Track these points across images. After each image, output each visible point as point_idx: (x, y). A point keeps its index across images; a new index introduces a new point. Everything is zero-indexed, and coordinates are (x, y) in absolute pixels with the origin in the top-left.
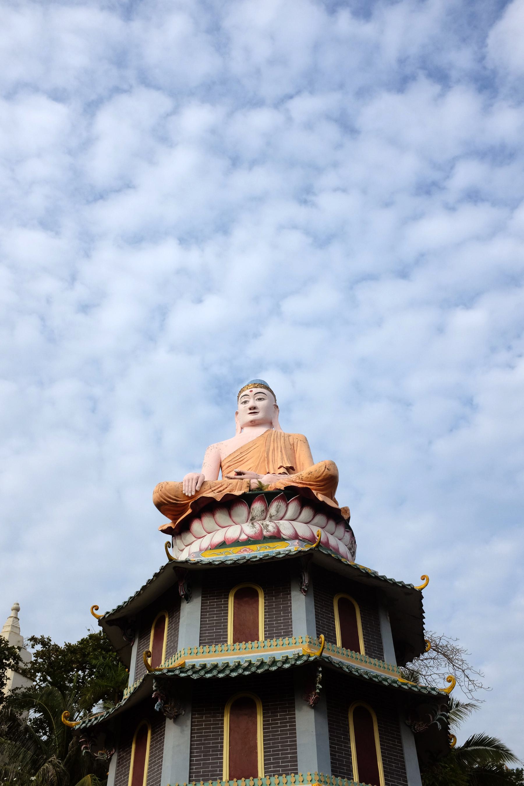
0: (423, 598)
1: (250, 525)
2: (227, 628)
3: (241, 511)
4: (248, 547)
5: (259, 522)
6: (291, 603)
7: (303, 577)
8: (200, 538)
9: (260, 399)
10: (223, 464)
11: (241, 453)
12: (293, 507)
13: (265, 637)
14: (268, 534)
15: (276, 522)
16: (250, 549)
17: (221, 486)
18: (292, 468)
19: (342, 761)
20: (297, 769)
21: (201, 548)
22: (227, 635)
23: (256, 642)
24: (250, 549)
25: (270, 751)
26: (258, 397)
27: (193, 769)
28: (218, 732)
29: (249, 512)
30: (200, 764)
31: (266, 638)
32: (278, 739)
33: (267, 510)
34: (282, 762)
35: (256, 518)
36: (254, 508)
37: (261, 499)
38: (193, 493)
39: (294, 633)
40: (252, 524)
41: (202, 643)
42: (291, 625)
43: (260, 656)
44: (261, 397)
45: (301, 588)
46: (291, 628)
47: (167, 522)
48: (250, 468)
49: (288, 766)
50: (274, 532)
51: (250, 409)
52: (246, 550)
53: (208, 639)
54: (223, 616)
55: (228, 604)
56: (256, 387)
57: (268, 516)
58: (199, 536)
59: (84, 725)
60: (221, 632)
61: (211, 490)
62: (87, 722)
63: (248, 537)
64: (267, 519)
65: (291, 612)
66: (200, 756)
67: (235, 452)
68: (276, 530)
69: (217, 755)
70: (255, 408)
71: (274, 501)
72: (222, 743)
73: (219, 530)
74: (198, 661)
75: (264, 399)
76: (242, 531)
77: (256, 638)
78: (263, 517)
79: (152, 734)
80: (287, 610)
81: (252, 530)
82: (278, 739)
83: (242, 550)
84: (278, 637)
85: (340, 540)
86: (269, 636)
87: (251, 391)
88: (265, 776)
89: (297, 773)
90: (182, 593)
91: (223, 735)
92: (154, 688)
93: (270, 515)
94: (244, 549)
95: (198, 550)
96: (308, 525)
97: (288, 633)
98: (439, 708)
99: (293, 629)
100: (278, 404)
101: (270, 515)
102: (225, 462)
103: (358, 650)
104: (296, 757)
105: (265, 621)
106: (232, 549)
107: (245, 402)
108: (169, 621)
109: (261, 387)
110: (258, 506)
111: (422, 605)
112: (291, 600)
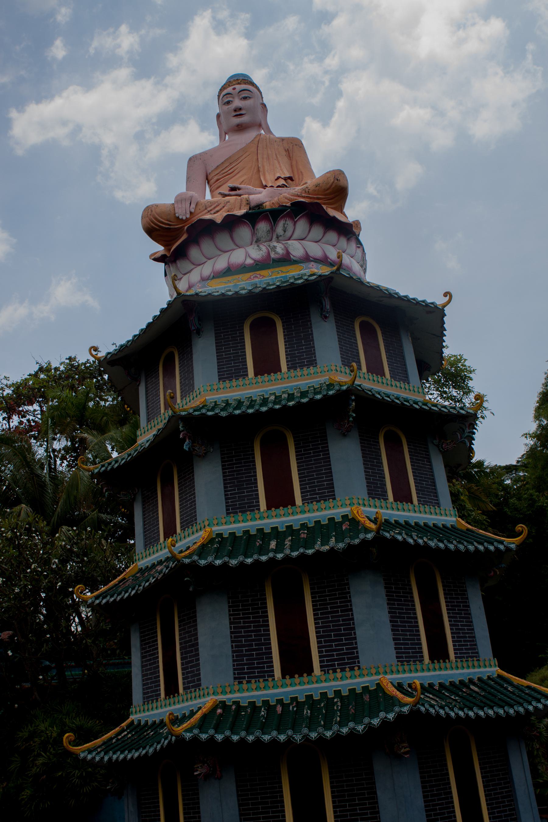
0: (446, 315)
1: (256, 247)
2: (246, 361)
4: (258, 272)
6: (312, 331)
7: (324, 303)
8: (199, 265)
9: (245, 98)
10: (210, 178)
11: (230, 164)
12: (302, 225)
13: (288, 368)
14: (277, 256)
15: (284, 242)
16: (260, 275)
17: (218, 205)
18: (291, 178)
19: (377, 484)
20: (334, 495)
21: (202, 276)
22: (247, 368)
23: (279, 373)
24: (260, 275)
25: (305, 480)
26: (243, 96)
27: (228, 502)
28: (250, 466)
30: (235, 498)
31: (289, 369)
32: (312, 468)
33: (272, 229)
34: (319, 490)
35: (262, 239)
36: (258, 228)
38: (188, 216)
39: (318, 362)
40: (258, 246)
41: (222, 378)
42: (315, 353)
43: (285, 388)
44: (246, 95)
45: (321, 314)
46: (315, 357)
47: (159, 249)
49: (325, 493)
50: (283, 254)
51: (235, 111)
52: (256, 277)
53: (227, 374)
54: (240, 349)
56: (239, 84)
57: (275, 237)
59: (103, 469)
60: (240, 366)
61: (206, 211)
62: (106, 465)
63: (255, 261)
64: (273, 240)
65: (313, 340)
66: (235, 490)
67: (222, 163)
68: (285, 252)
69: (252, 487)
70: (240, 109)
71: (280, 219)
72: (256, 476)
73: (220, 255)
75: (250, 98)
76: (247, 255)
77: (277, 369)
78: (268, 238)
79: (178, 473)
80: (309, 338)
81: (258, 253)
82: (312, 468)
83: (252, 277)
84: (302, 367)
85: (352, 257)
86: (292, 366)
87: (234, 89)
88: (303, 504)
89: (334, 499)
90: (193, 328)
91: (255, 468)
92: (181, 428)
93: (277, 235)
94: (254, 276)
95: (199, 278)
96: (319, 243)
97: (312, 362)
98: (467, 426)
99: (317, 358)
100: (264, 102)
101: (277, 235)
102: (213, 175)
103: (383, 374)
104: (333, 484)
105: (286, 352)
106: (241, 276)
107: (228, 103)
108: (179, 358)
109: (245, 84)
110: (263, 227)
111: (443, 323)
112: (311, 327)
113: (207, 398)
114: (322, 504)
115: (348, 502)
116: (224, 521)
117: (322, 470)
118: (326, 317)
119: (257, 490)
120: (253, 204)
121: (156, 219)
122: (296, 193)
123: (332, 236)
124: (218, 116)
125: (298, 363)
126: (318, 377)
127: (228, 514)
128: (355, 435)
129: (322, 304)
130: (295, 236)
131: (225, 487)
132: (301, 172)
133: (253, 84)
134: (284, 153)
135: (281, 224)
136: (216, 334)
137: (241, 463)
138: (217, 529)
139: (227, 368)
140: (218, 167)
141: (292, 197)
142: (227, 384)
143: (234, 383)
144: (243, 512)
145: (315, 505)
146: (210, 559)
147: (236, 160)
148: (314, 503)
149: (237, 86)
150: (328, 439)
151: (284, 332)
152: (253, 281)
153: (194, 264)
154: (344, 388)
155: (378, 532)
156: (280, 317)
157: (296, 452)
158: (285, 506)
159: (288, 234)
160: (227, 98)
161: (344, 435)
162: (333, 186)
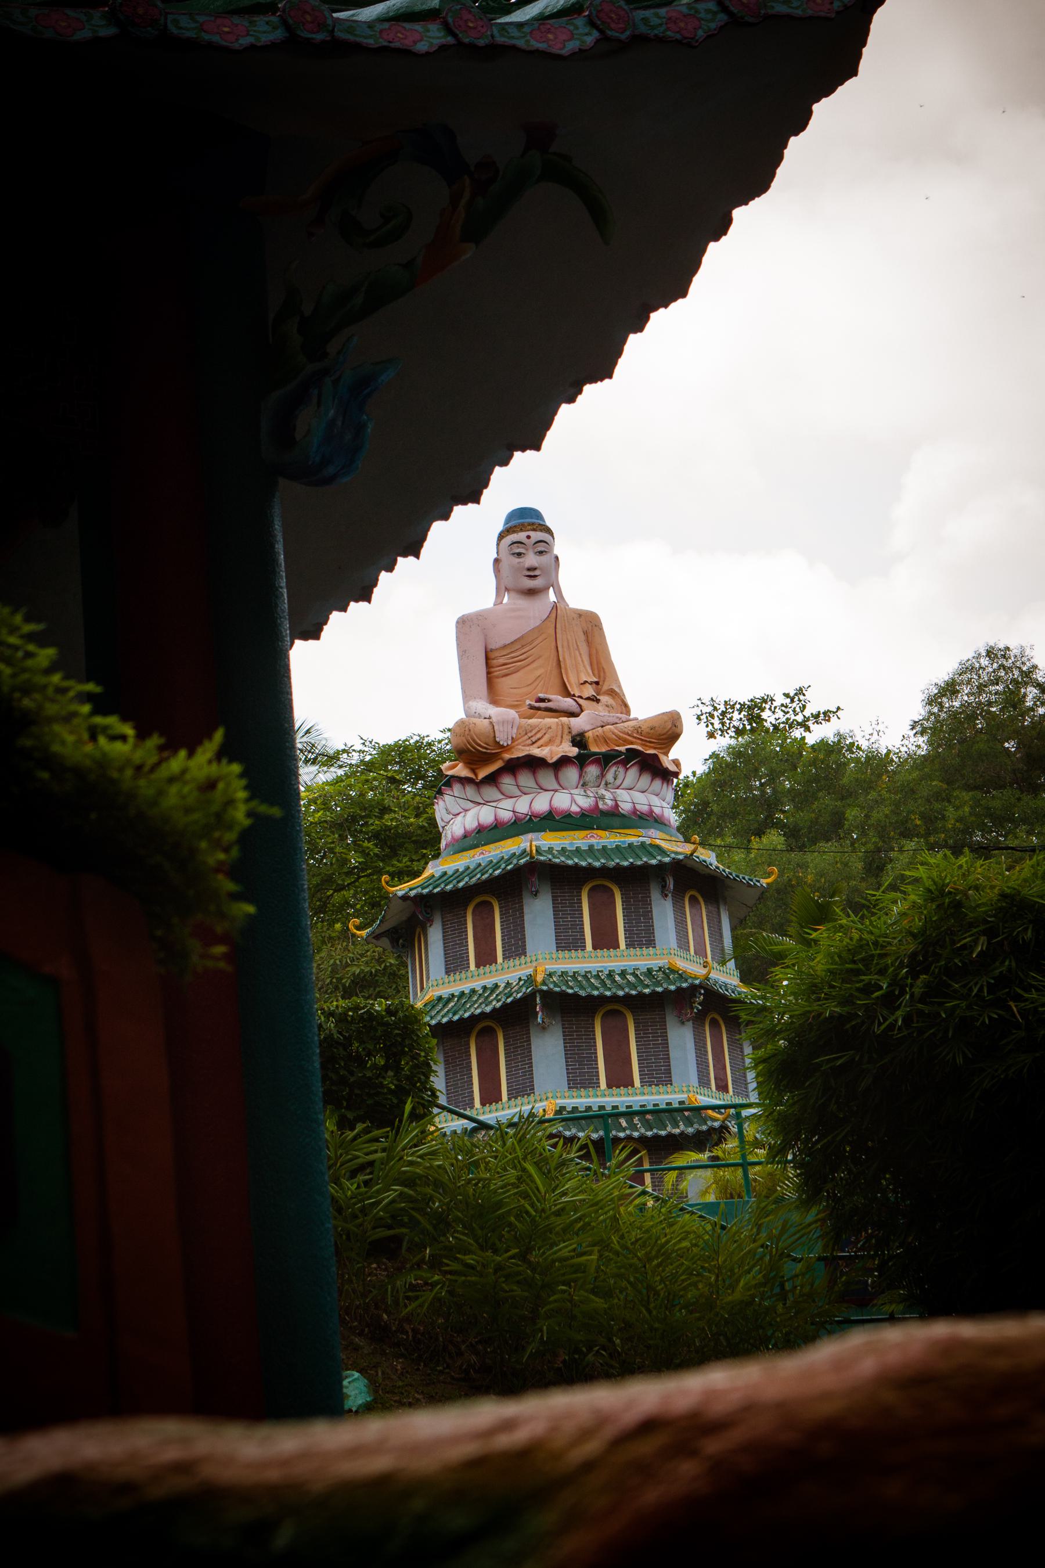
2: (583, 932)
3: (571, 774)
5: (593, 789)
6: (651, 908)
7: (668, 882)
8: (511, 797)
9: (541, 553)
10: (492, 655)
11: (523, 646)
12: (633, 772)
13: (626, 945)
14: (606, 807)
15: (612, 790)
16: (598, 836)
17: (539, 731)
20: (671, 1081)
22: (584, 939)
24: (598, 836)
25: (644, 1063)
28: (591, 1043)
29: (580, 776)
32: (651, 1052)
33: (602, 775)
35: (589, 784)
36: (588, 771)
37: (597, 762)
41: (559, 948)
42: (653, 933)
43: (624, 966)
44: (543, 549)
45: (662, 892)
46: (654, 937)
48: (539, 676)
50: (612, 806)
51: (529, 569)
52: (592, 836)
53: (565, 943)
54: (577, 918)
55: (581, 903)
56: (534, 530)
57: (603, 783)
58: (511, 795)
61: (526, 737)
63: (582, 809)
65: (652, 919)
67: (512, 643)
69: (592, 1064)
70: (535, 569)
74: (559, 967)
75: (546, 552)
76: (573, 800)
77: (616, 946)
78: (597, 784)
80: (648, 915)
82: (651, 1052)
84: (641, 946)
88: (642, 1086)
89: (671, 1084)
91: (596, 1046)
93: (606, 782)
96: (645, 793)
97: (650, 943)
99: (656, 938)
101: (606, 782)
105: (625, 927)
107: (519, 554)
108: (500, 911)
109: (541, 531)
110: (593, 771)
112: (651, 904)
113: (547, 967)
114: (662, 1089)
115: (685, 1089)
116: (567, 1094)
117: (660, 1055)
118: (666, 896)
119: (597, 1068)
120: (574, 733)
121: (474, 741)
122: (626, 730)
123: (657, 783)
124: (497, 561)
125: (636, 941)
126: (657, 959)
127: (569, 1088)
128: (690, 1023)
129: (665, 881)
130: (625, 785)
131: (566, 1062)
132: (603, 669)
133: (548, 531)
134: (583, 637)
135: (614, 769)
136: (552, 896)
137: (582, 1039)
138: (561, 1102)
139: (564, 936)
140: (505, 647)
141: (621, 735)
142: (567, 954)
143: (574, 953)
144: (585, 1088)
145: (654, 1089)
146: (574, 1131)
147: (530, 643)
148: (653, 1086)
149: (531, 533)
150: (667, 1022)
151: (623, 905)
152: (589, 841)
153: (503, 794)
154: (697, 982)
155: (723, 1122)
156: (619, 888)
157: (636, 1034)
158: (626, 1086)
159: (618, 782)
160: (518, 547)
161: (683, 1023)
162: (670, 732)
